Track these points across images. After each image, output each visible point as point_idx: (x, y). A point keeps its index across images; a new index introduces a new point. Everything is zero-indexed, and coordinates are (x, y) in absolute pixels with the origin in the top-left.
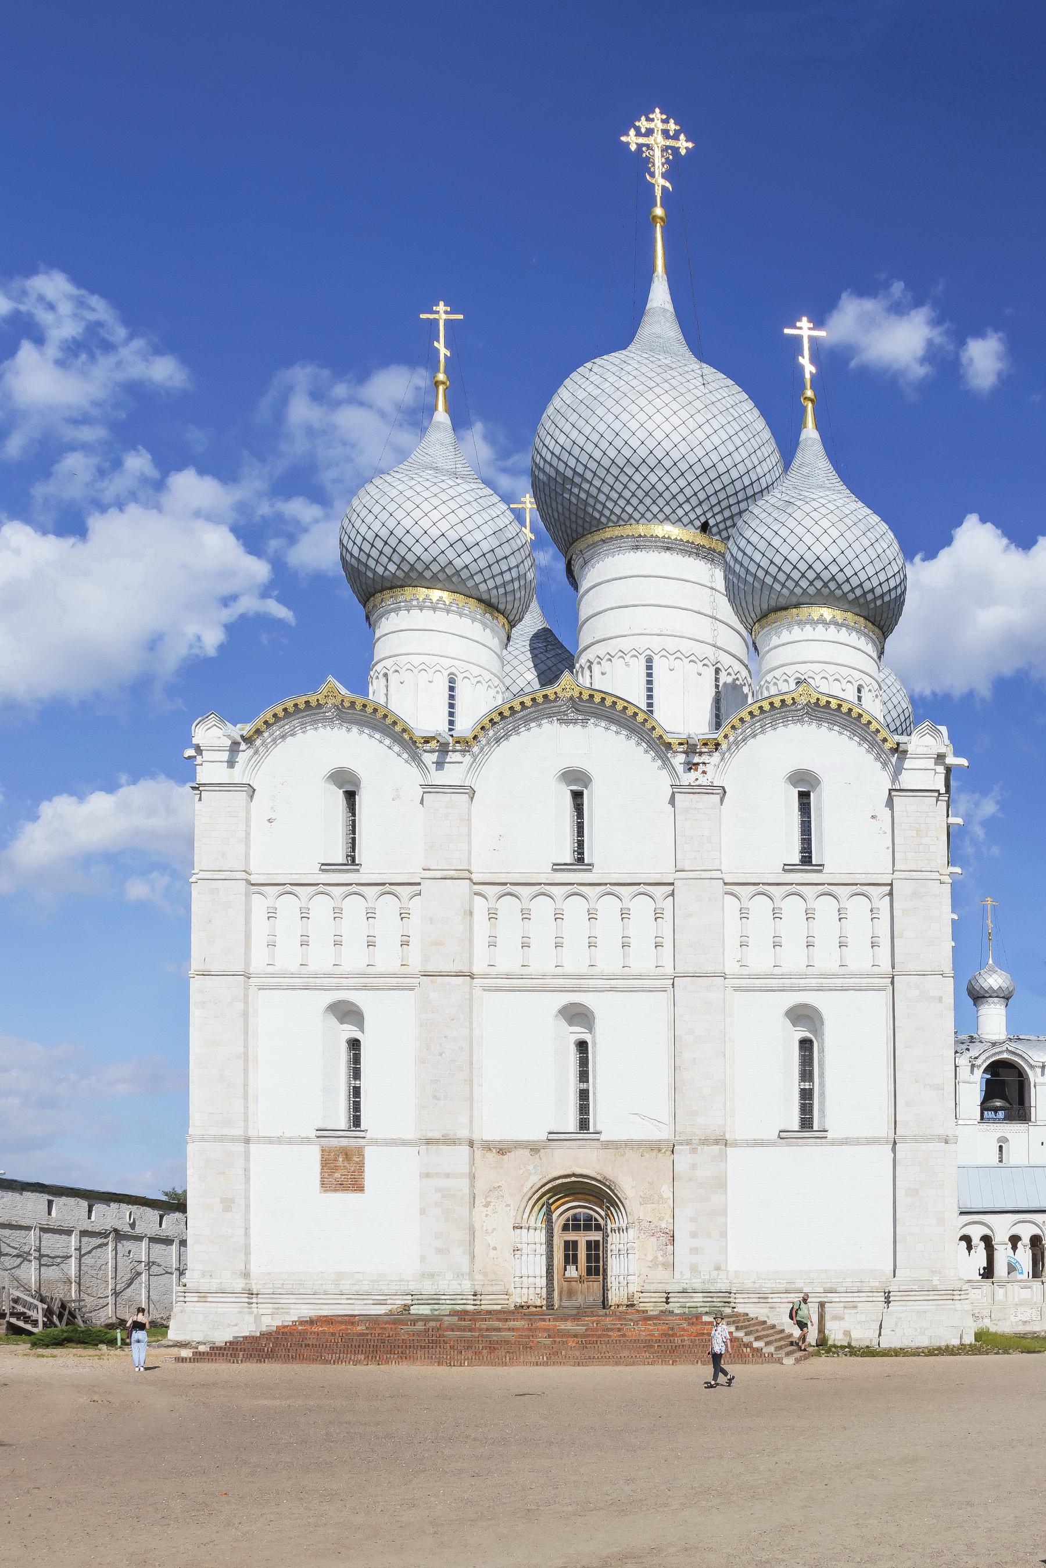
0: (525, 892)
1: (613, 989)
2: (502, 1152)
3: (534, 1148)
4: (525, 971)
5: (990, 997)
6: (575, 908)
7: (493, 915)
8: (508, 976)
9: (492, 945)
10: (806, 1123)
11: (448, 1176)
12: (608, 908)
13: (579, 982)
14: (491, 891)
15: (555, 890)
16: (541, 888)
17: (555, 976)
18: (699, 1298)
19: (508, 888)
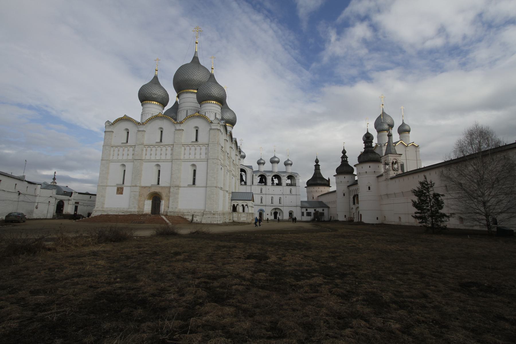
0: (151, 147)
1: (164, 162)
2: (144, 188)
3: (149, 187)
4: (151, 159)
6: (159, 149)
7: (146, 150)
8: (148, 160)
9: (146, 155)
10: (194, 183)
11: (135, 192)
12: (164, 149)
13: (158, 161)
14: (146, 146)
15: (156, 146)
16: (154, 146)
17: (155, 160)
18: (172, 213)
19: (149, 146)
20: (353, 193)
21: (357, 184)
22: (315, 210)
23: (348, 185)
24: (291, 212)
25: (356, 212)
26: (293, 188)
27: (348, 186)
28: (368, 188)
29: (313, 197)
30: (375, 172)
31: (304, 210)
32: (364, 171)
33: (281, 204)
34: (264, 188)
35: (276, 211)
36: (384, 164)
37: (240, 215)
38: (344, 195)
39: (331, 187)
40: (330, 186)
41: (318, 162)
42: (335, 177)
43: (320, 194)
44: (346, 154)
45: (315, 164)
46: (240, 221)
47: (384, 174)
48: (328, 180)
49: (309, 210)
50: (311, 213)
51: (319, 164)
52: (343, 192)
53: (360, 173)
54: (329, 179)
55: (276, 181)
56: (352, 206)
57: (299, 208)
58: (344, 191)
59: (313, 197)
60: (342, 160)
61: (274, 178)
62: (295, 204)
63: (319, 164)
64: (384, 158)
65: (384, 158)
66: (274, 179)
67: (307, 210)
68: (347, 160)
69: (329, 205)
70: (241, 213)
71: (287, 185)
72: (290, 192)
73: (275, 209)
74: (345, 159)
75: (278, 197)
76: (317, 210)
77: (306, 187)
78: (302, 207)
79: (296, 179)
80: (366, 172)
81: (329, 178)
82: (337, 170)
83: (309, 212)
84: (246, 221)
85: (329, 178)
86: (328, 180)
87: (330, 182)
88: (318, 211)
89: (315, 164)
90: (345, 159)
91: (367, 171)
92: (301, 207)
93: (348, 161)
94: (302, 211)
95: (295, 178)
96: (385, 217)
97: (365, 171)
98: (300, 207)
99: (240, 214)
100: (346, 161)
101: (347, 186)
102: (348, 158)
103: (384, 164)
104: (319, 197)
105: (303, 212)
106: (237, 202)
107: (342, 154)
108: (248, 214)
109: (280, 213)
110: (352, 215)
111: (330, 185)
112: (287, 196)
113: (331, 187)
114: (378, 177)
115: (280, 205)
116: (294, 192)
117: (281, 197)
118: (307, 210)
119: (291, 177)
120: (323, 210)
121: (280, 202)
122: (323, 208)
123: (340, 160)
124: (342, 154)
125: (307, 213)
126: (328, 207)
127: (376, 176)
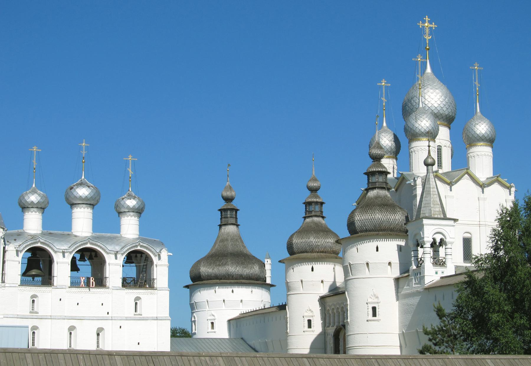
5: (32, 207)
34: (42, 292)
61: (78, 256)
77: (187, 287)
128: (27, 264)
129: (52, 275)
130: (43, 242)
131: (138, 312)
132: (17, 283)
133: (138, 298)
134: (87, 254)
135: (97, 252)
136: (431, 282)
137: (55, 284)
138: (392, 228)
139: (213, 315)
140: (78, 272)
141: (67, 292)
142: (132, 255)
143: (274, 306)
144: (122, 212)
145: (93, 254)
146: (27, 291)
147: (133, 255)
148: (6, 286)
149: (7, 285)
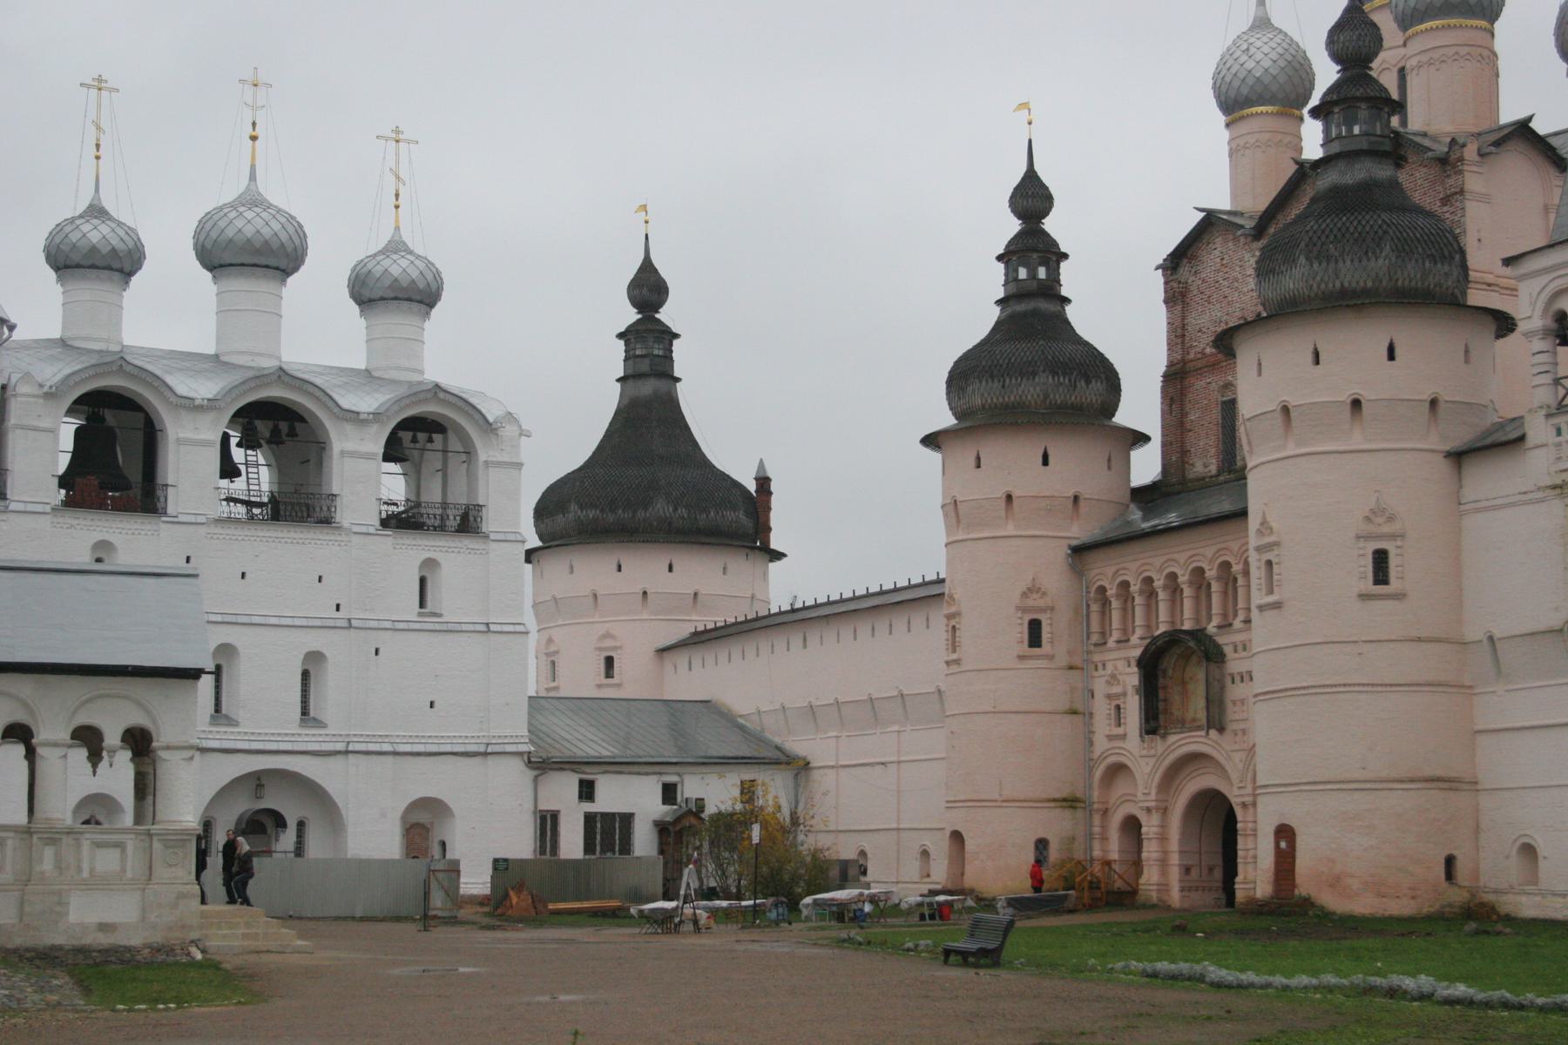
20: (1163, 607)
21: (1242, 514)
22: (669, 793)
23: (1080, 532)
24: (422, 817)
25: (1164, 811)
26: (451, 554)
27: (1080, 551)
28: (1368, 562)
29: (609, 661)
30: (1434, 403)
31: (561, 792)
32: (1424, 397)
33: (319, 724)
35: (267, 804)
36: (1546, 333)
37: (58, 858)
38: (1035, 628)
39: (777, 556)
40: (773, 546)
41: (657, 305)
42: (934, 457)
43: (685, 631)
44: (1050, 224)
45: (631, 315)
46: (59, 939)
47: (1538, 430)
48: (752, 487)
49: (613, 795)
50: (627, 819)
51: (665, 315)
52: (1030, 602)
53: (1286, 410)
54: (764, 483)
55: (259, 476)
56: (1133, 747)
57: (515, 775)
58: (1035, 601)
59: (609, 661)
60: (1010, 279)
62: (467, 734)
63: (665, 315)
64: (1546, 270)
65: (1546, 270)
66: (238, 455)
67: (587, 791)
68: (1054, 279)
69: (798, 745)
70: (66, 840)
71: (402, 521)
72: (422, 604)
73: (257, 781)
74: (1023, 273)
75: (295, 647)
76: (692, 787)
78: (542, 765)
79: (483, 455)
80: (1356, 404)
81: (761, 465)
82: (963, 375)
83: (608, 817)
84: (136, 941)
85: (761, 465)
86: (752, 487)
87: (768, 508)
88: (700, 803)
89: (631, 315)
90: (1042, 273)
91: (1366, 394)
92: (530, 763)
93: (1064, 292)
94: (543, 806)
95: (469, 453)
96: (1529, 851)
97: (1345, 397)
98: (517, 765)
99: (49, 852)
100: (1051, 292)
101: (1062, 551)
102: (1064, 265)
103: (1546, 333)
104: (681, 658)
105: (555, 816)
106: (25, 705)
107: (1014, 226)
108: (157, 845)
109: (301, 825)
110: (1104, 839)
111: (766, 542)
112: (385, 640)
113: (777, 556)
114: (1458, 457)
115: (311, 739)
116: (451, 599)
117: (237, 644)
118: (587, 791)
119: (421, 436)
120: (748, 790)
121: (305, 711)
122: (748, 774)
123: (993, 280)
124: (1014, 226)
125: (590, 819)
126: (800, 768)
127: (1448, 448)
128: (70, 455)
129: (160, 481)
130: (133, 375)
131: (430, 607)
132: (48, 501)
133: (430, 564)
134: (263, 428)
135: (302, 420)
136: (1508, 496)
137: (170, 510)
138: (1447, 289)
139: (612, 637)
140: (232, 482)
141: (209, 536)
142: (401, 434)
143: (926, 579)
144: (374, 300)
145: (284, 426)
146: (78, 527)
147: (406, 436)
148: (11, 508)
149: (13, 506)
